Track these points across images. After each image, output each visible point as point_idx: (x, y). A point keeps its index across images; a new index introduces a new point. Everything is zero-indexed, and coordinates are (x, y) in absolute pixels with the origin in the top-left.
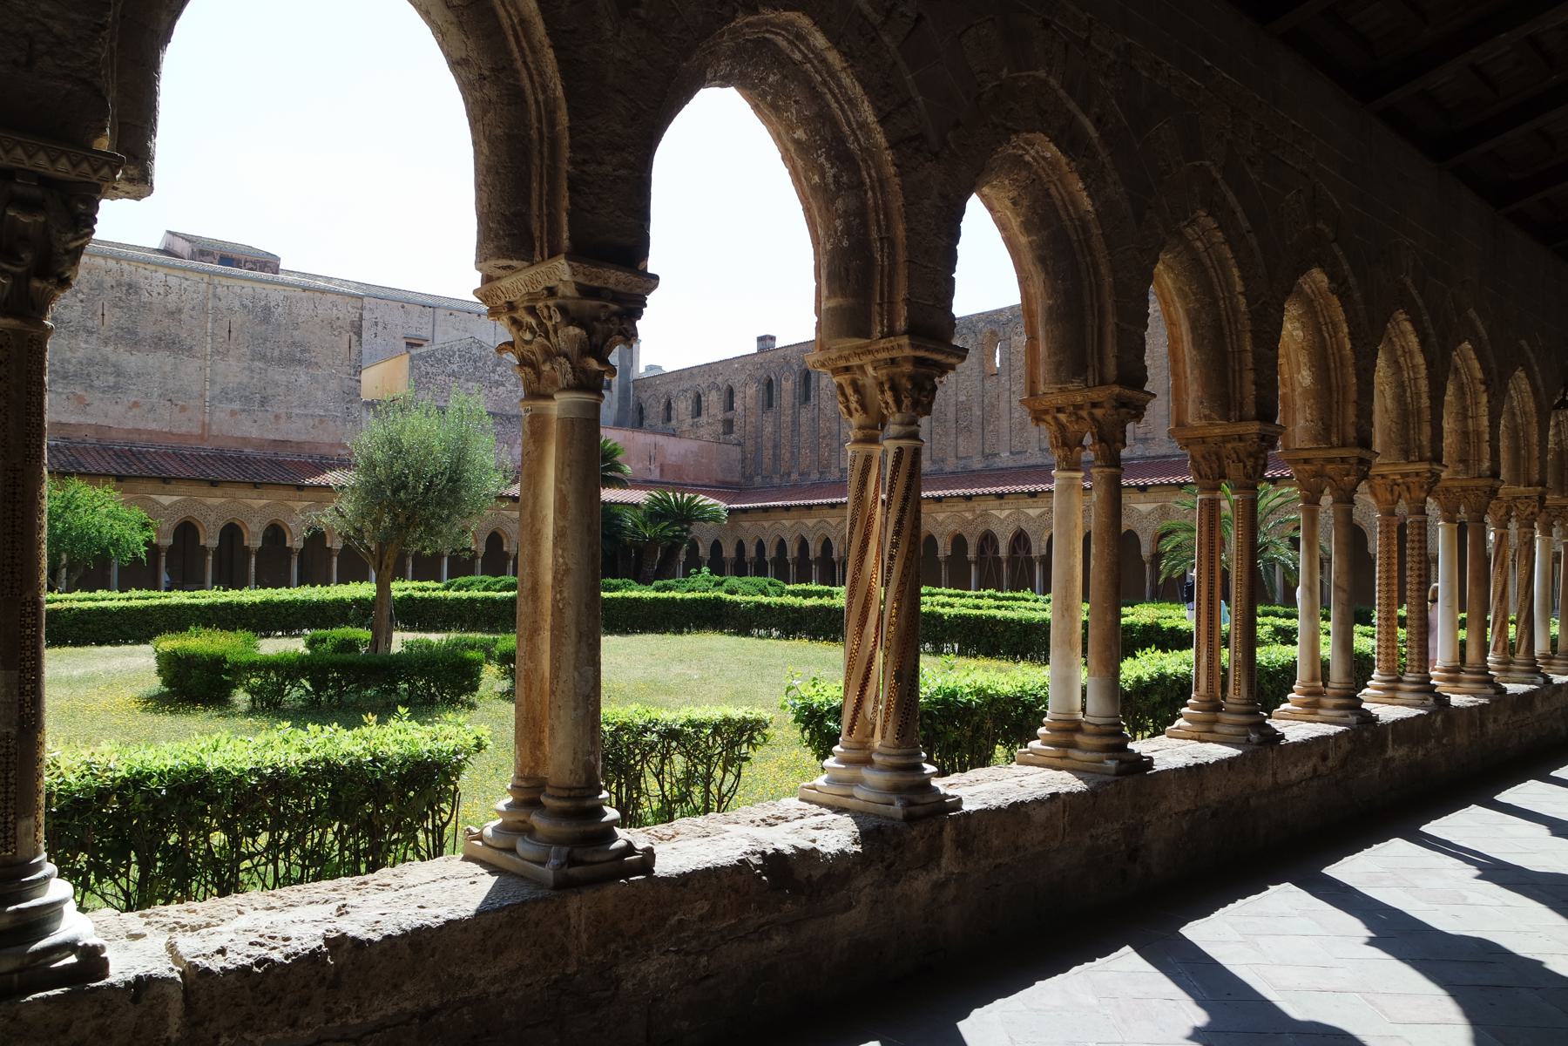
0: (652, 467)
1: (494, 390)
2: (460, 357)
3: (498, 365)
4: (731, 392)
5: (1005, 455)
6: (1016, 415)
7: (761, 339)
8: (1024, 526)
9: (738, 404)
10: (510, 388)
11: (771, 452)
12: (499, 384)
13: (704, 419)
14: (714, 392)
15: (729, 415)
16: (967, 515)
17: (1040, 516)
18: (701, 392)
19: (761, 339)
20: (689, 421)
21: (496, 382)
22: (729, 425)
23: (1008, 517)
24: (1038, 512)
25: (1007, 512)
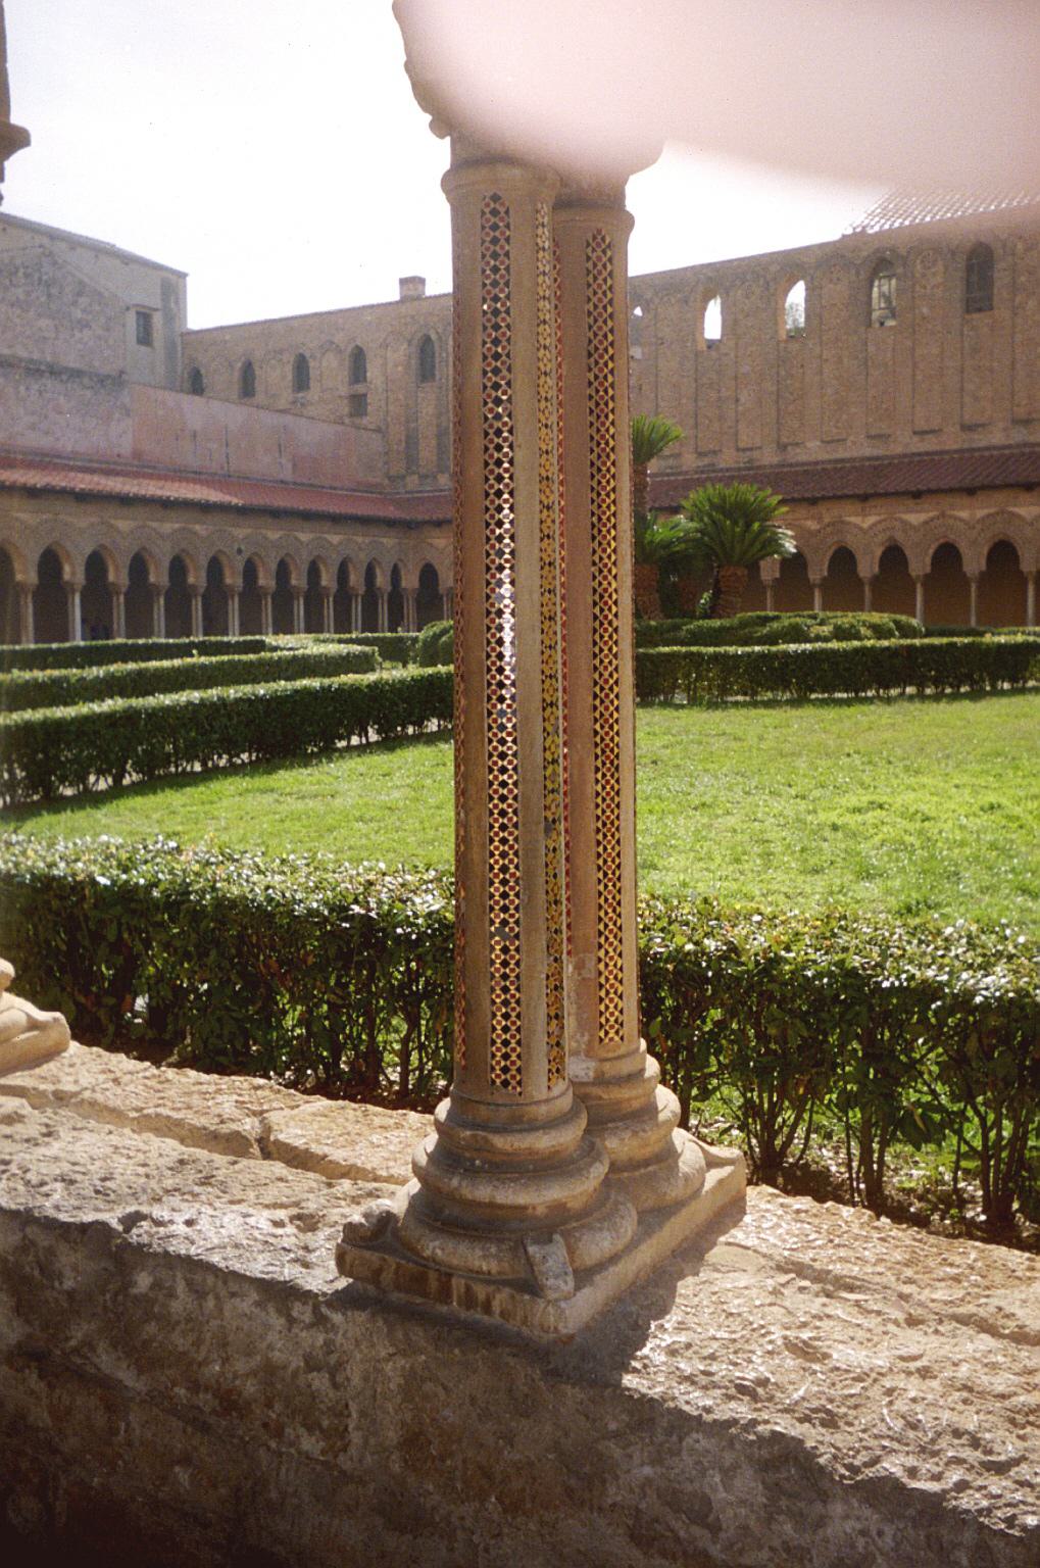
0: (284, 461)
1: (78, 335)
2: (27, 276)
3: (79, 294)
4: (358, 359)
5: (814, 444)
6: (829, 391)
7: (404, 282)
8: (900, 537)
9: (373, 372)
10: (100, 332)
11: (434, 442)
12: (84, 325)
13: (314, 394)
14: (330, 356)
15: (360, 388)
16: (809, 523)
17: (926, 523)
18: (307, 355)
19: (404, 282)
20: (286, 397)
21: (79, 322)
22: (358, 403)
23: (874, 525)
24: (922, 517)
25: (871, 520)
